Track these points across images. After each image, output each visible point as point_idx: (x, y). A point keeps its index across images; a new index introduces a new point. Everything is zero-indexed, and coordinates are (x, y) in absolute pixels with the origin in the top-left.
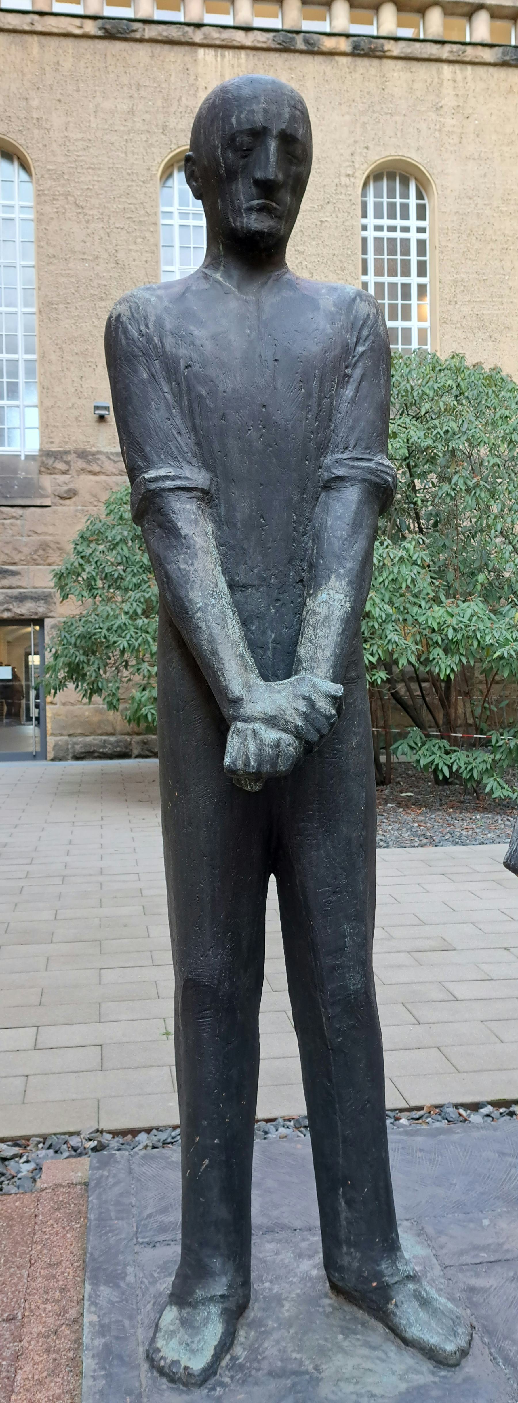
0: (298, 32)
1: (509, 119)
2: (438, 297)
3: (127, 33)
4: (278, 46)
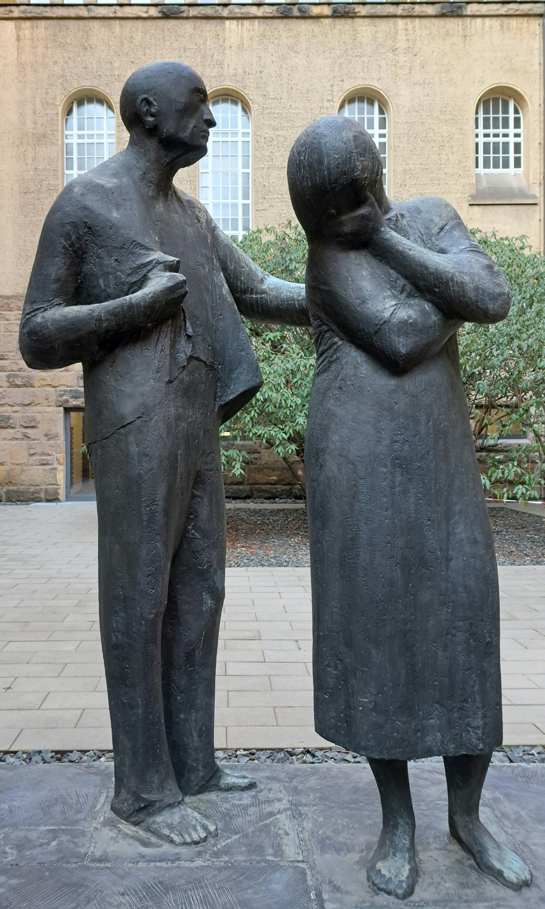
0: (294, 4)
1: (446, 54)
2: (392, 183)
3: (178, 14)
4: (280, 15)
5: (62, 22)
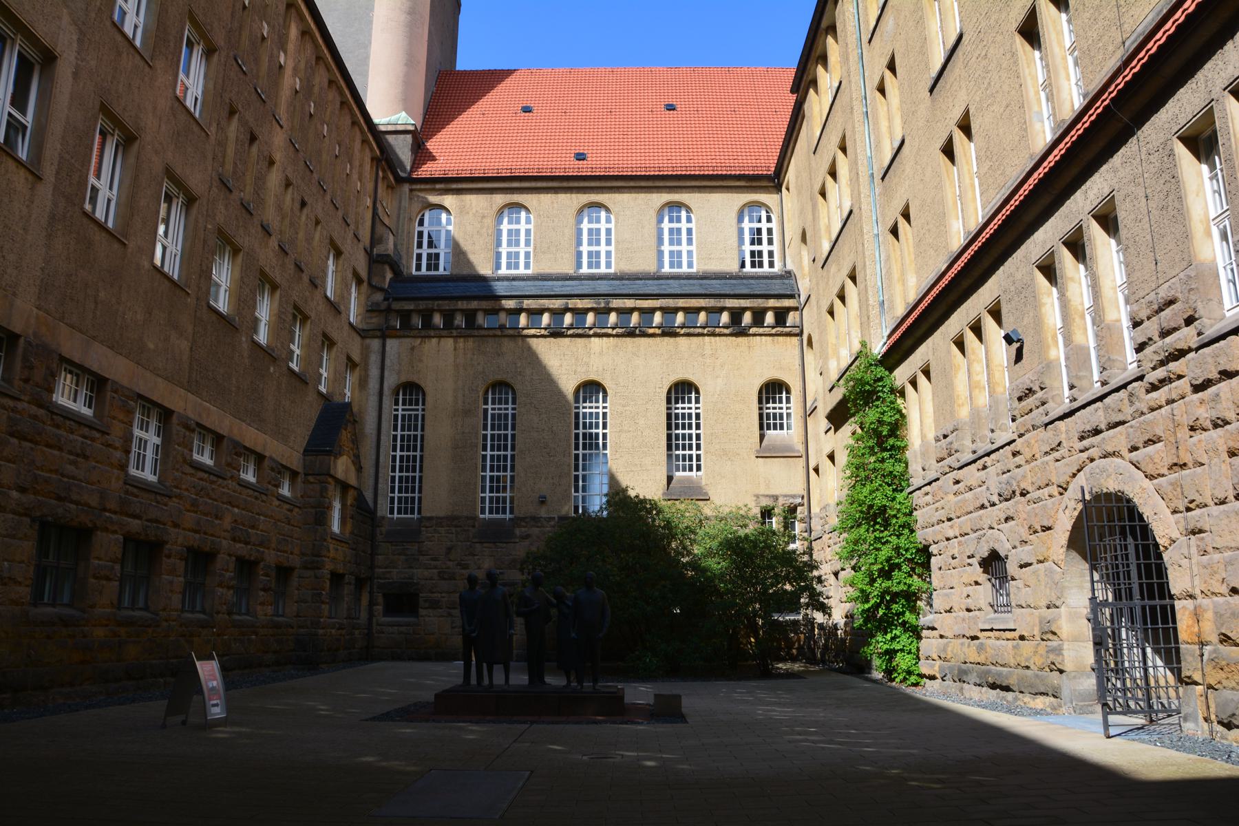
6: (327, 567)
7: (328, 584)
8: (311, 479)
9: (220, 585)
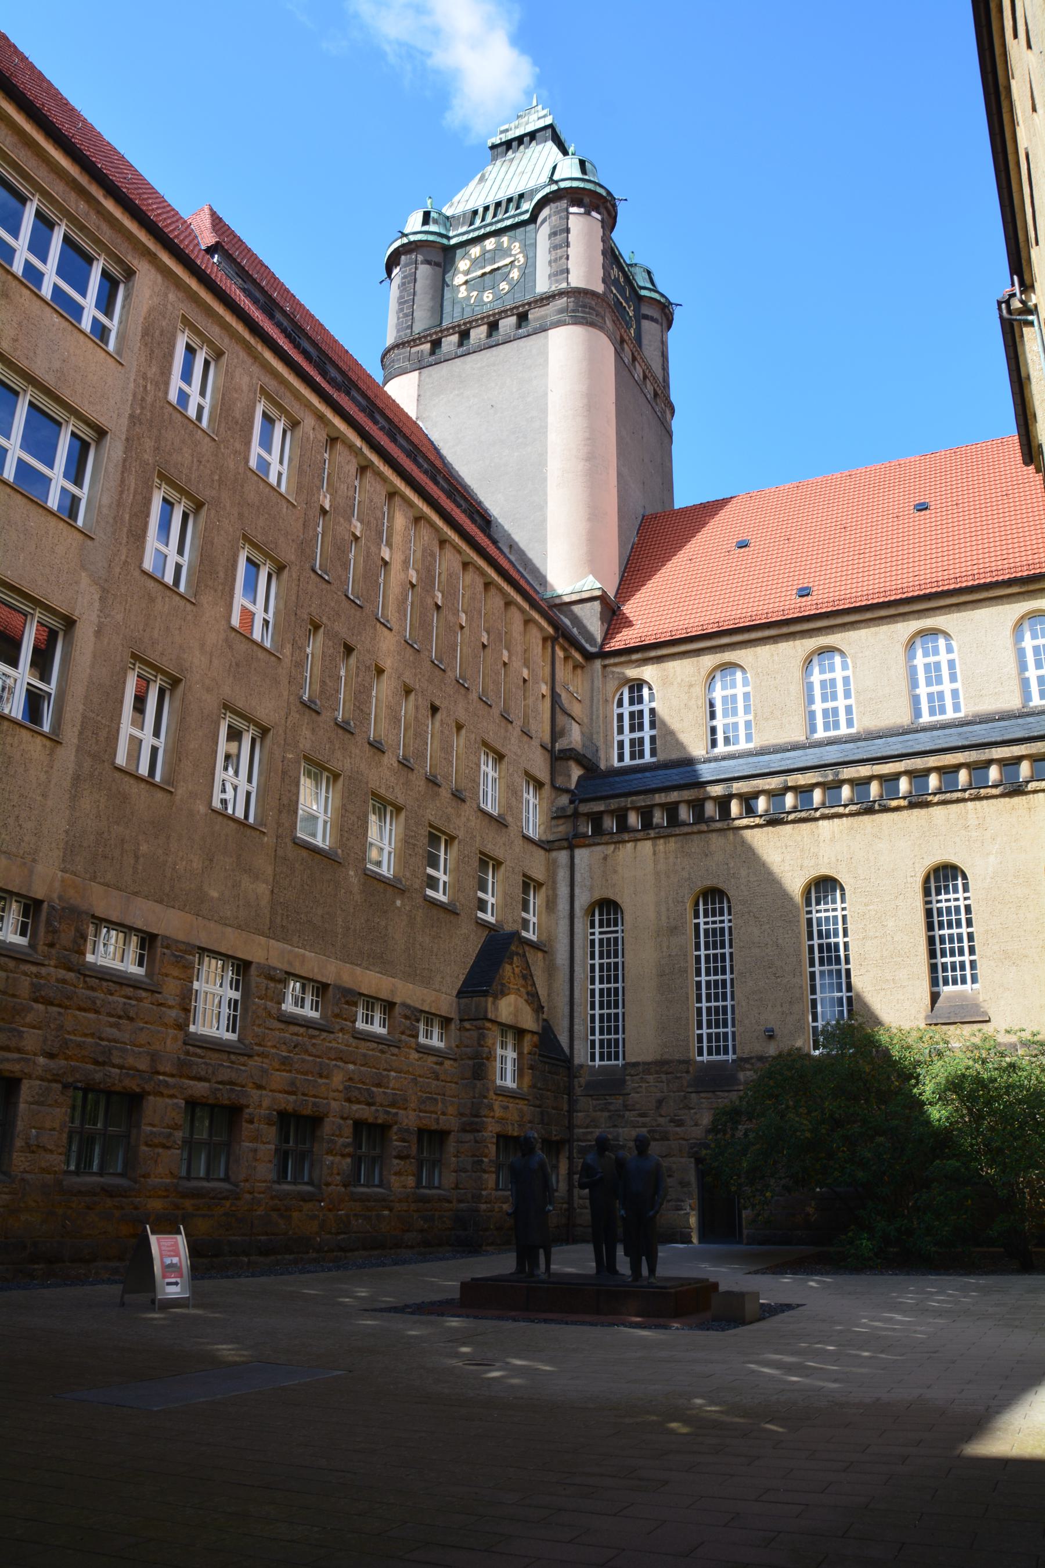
5: (688, 837)
6: (490, 1129)
7: (493, 1148)
8: (467, 1025)
9: (329, 1152)
